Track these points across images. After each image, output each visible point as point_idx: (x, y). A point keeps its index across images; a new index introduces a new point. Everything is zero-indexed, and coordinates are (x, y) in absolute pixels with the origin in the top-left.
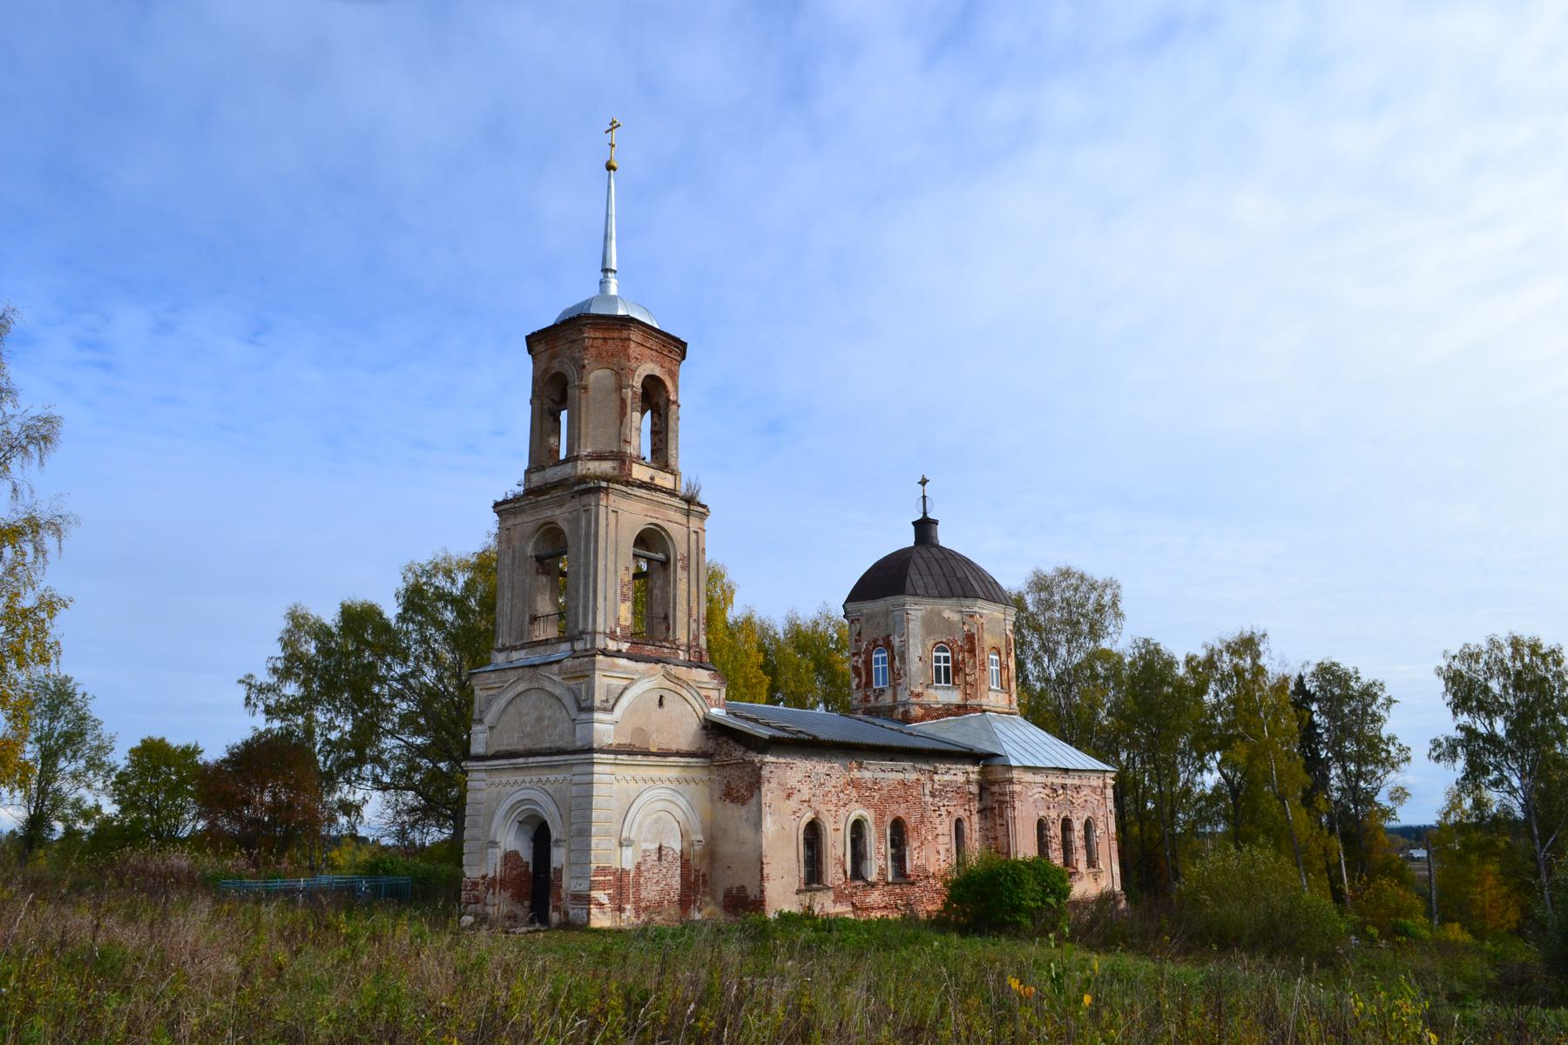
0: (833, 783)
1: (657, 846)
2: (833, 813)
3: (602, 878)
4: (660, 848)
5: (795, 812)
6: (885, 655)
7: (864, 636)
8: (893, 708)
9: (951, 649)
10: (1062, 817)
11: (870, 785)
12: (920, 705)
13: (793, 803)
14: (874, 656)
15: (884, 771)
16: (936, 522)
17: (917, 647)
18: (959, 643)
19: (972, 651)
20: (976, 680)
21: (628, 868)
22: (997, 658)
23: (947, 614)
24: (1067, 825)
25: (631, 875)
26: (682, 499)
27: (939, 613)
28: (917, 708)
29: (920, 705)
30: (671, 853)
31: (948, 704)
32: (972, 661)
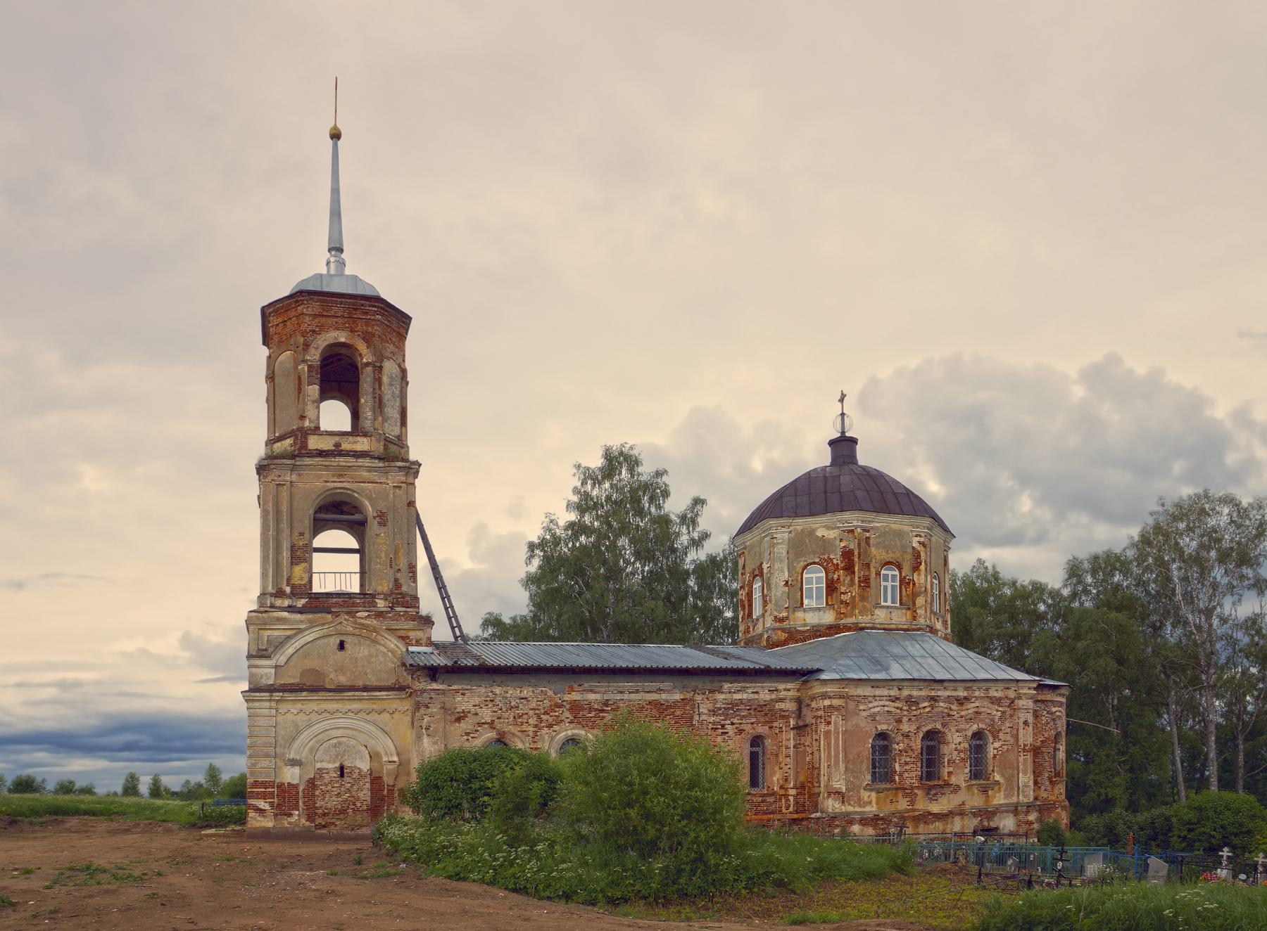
0: (533, 705)
1: (337, 765)
2: (531, 734)
3: (263, 790)
4: (342, 768)
5: (467, 734)
6: (760, 584)
7: (747, 568)
8: (761, 635)
9: (825, 569)
10: (925, 729)
11: (596, 706)
12: (783, 630)
13: (465, 725)
14: (754, 587)
15: (621, 692)
16: (853, 441)
17: (782, 571)
18: (835, 561)
19: (849, 568)
20: (852, 598)
21: (295, 782)
22: (897, 573)
23: (819, 533)
24: (933, 739)
25: (301, 788)
26: (373, 457)
27: (812, 532)
28: (779, 632)
29: (783, 630)
30: (357, 771)
31: (818, 625)
32: (849, 578)
